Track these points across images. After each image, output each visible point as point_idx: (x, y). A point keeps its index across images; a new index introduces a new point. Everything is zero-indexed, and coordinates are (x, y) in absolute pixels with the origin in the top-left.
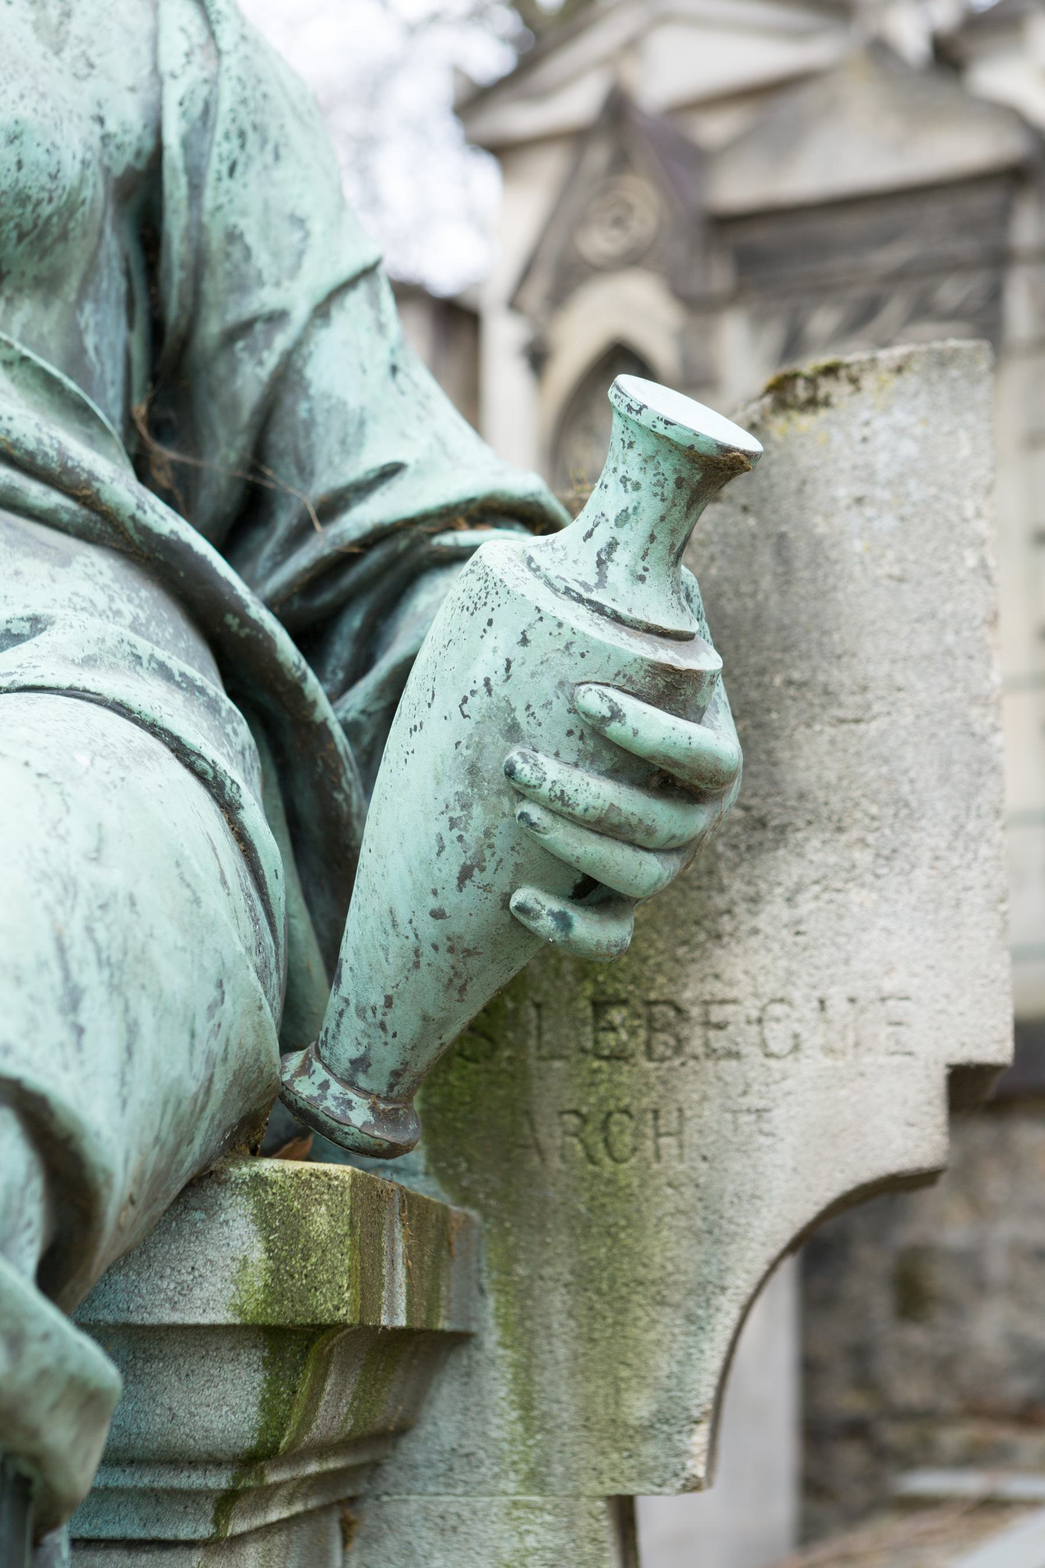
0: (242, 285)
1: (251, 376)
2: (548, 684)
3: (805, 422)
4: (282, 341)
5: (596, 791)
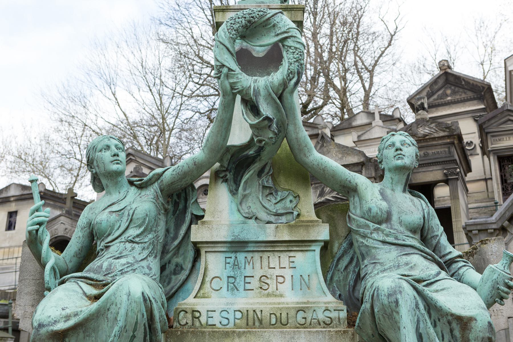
0: (433, 232)
1: (434, 242)
2: (501, 279)
3: (485, 246)
4: (438, 238)
5: (506, 290)
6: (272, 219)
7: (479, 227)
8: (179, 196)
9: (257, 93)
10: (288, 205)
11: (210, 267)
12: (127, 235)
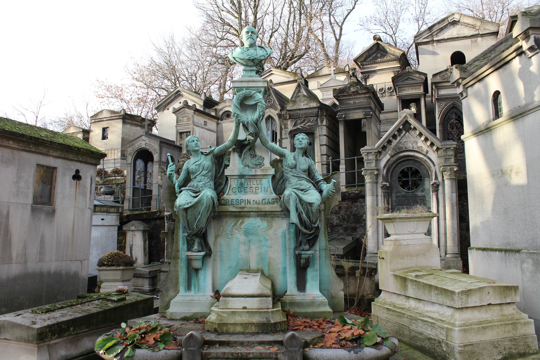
6: (254, 166)
7: (367, 151)
8: (220, 157)
9: (248, 123)
10: (260, 161)
11: (232, 184)
12: (202, 173)
